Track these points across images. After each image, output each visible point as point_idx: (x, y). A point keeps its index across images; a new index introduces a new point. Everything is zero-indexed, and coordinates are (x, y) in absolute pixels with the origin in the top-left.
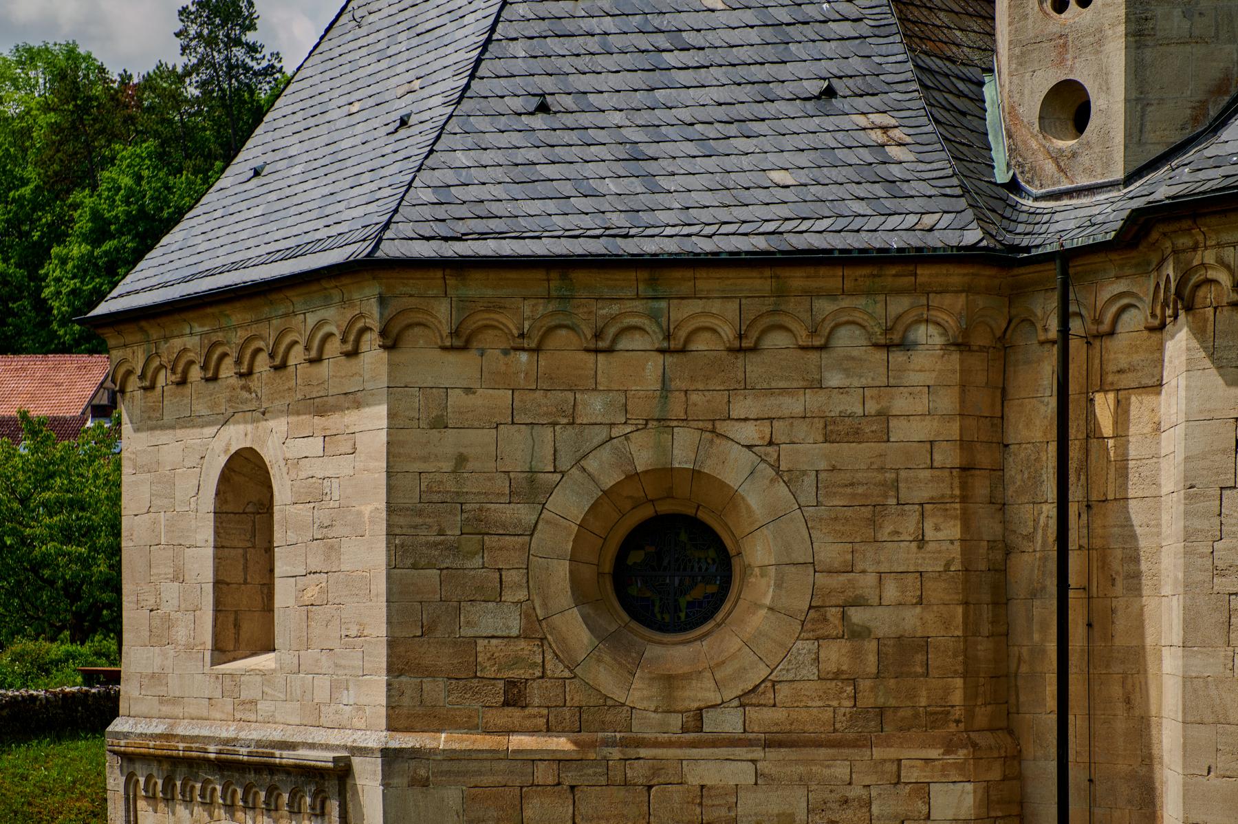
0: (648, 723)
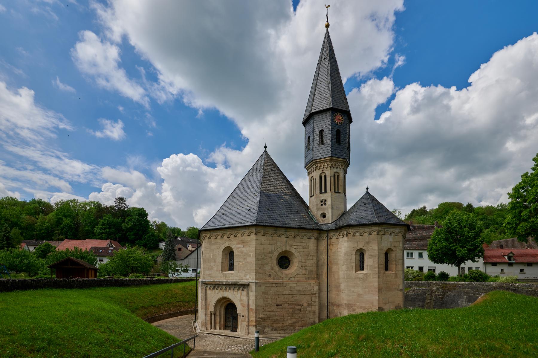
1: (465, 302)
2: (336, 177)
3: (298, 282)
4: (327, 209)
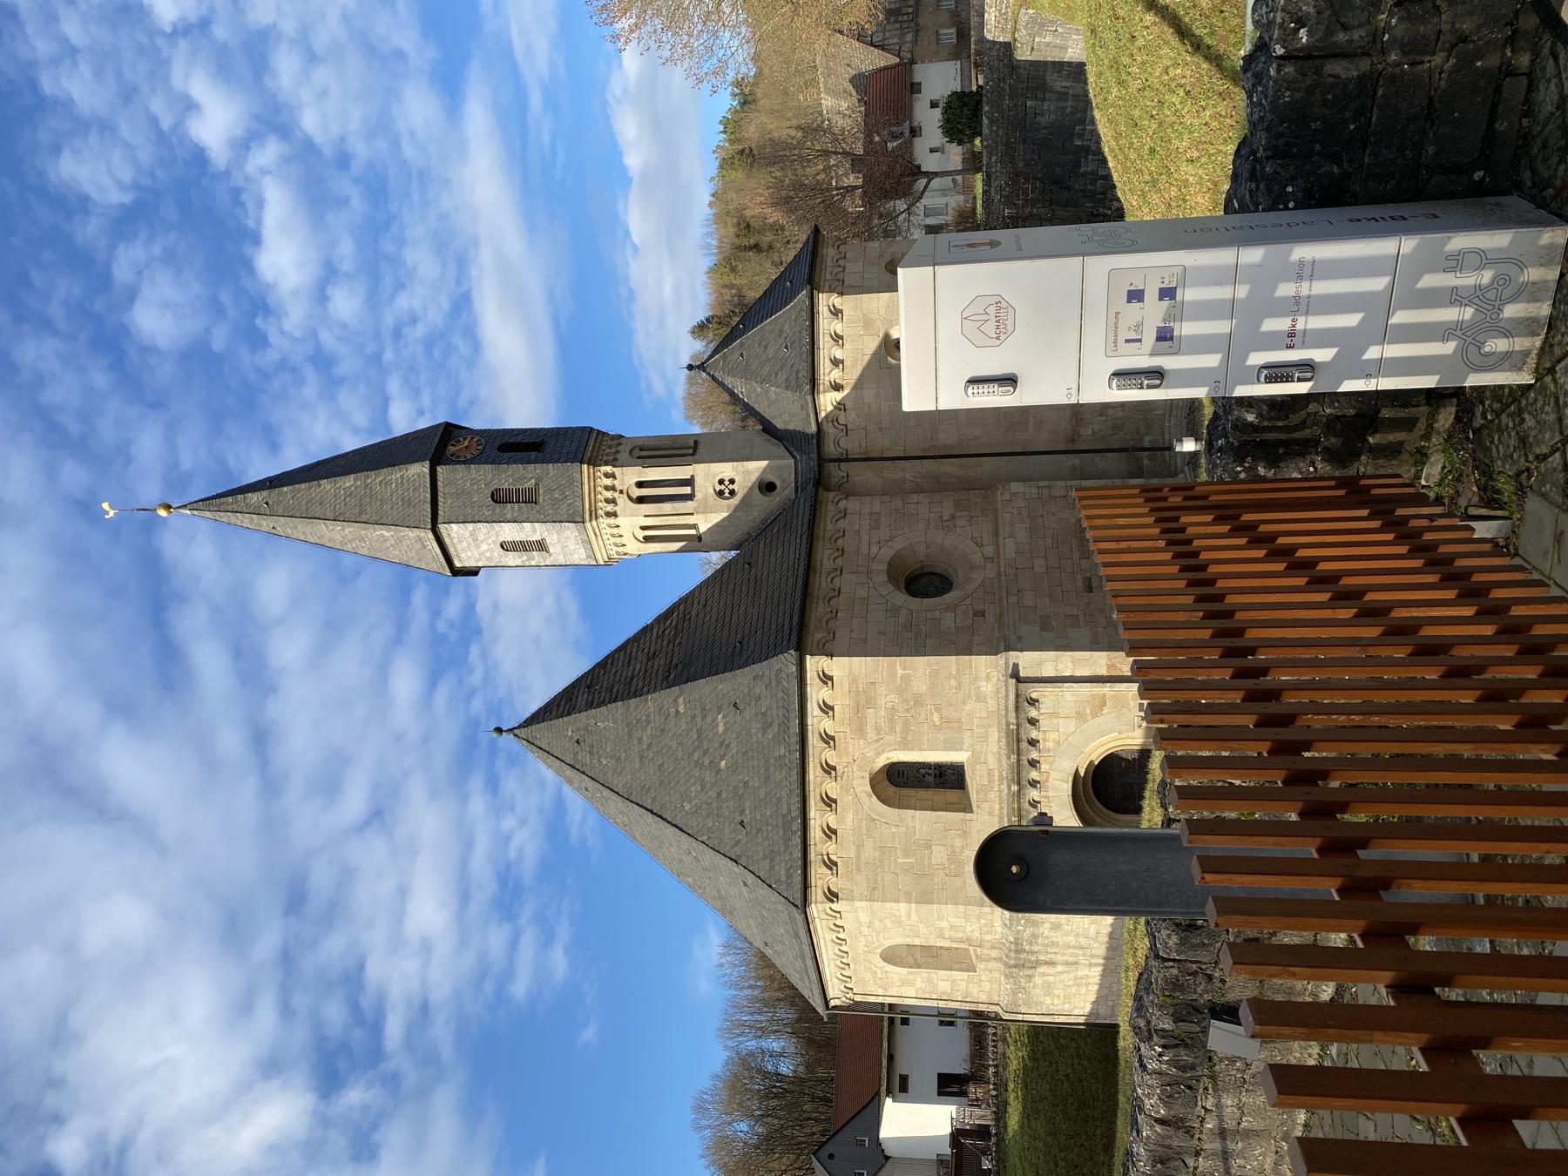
0: (990, 571)
1: (1044, 100)
3: (998, 535)
4: (747, 472)
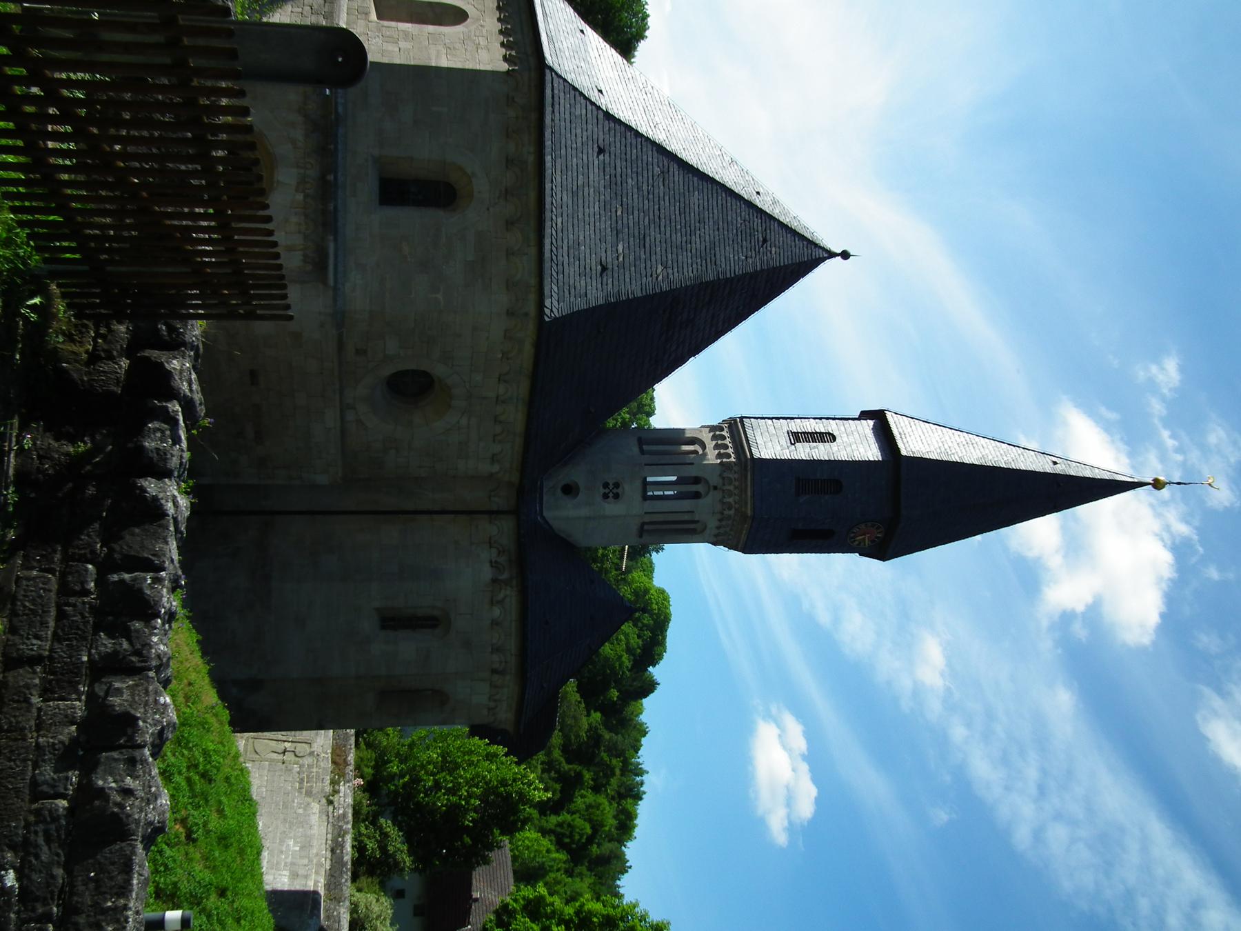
2: (692, 526)
